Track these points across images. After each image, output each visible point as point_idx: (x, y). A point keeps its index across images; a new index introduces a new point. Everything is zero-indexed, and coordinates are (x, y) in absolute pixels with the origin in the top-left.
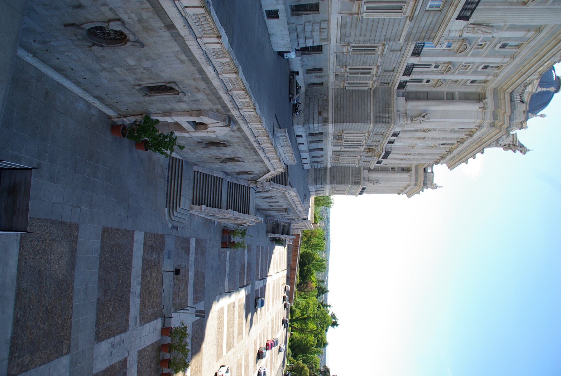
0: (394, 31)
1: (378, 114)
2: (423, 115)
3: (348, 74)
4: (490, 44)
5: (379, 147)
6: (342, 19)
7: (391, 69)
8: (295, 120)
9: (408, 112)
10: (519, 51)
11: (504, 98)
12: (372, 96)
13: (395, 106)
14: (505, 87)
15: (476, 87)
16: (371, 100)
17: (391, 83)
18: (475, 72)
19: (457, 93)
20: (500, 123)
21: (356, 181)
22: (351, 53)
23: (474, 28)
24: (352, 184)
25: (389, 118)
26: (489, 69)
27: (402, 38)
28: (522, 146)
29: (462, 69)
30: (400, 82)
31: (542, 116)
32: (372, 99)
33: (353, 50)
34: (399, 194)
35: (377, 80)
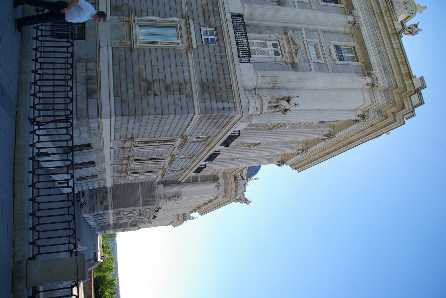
1: (145, 199)
2: (177, 196)
5: (148, 214)
8: (83, 210)
11: (231, 178)
12: (139, 186)
13: (157, 192)
14: (230, 172)
16: (139, 189)
19: (199, 177)
20: (230, 195)
21: (133, 224)
25: (153, 201)
28: (246, 199)
31: (256, 179)
32: (139, 188)
34: (167, 225)
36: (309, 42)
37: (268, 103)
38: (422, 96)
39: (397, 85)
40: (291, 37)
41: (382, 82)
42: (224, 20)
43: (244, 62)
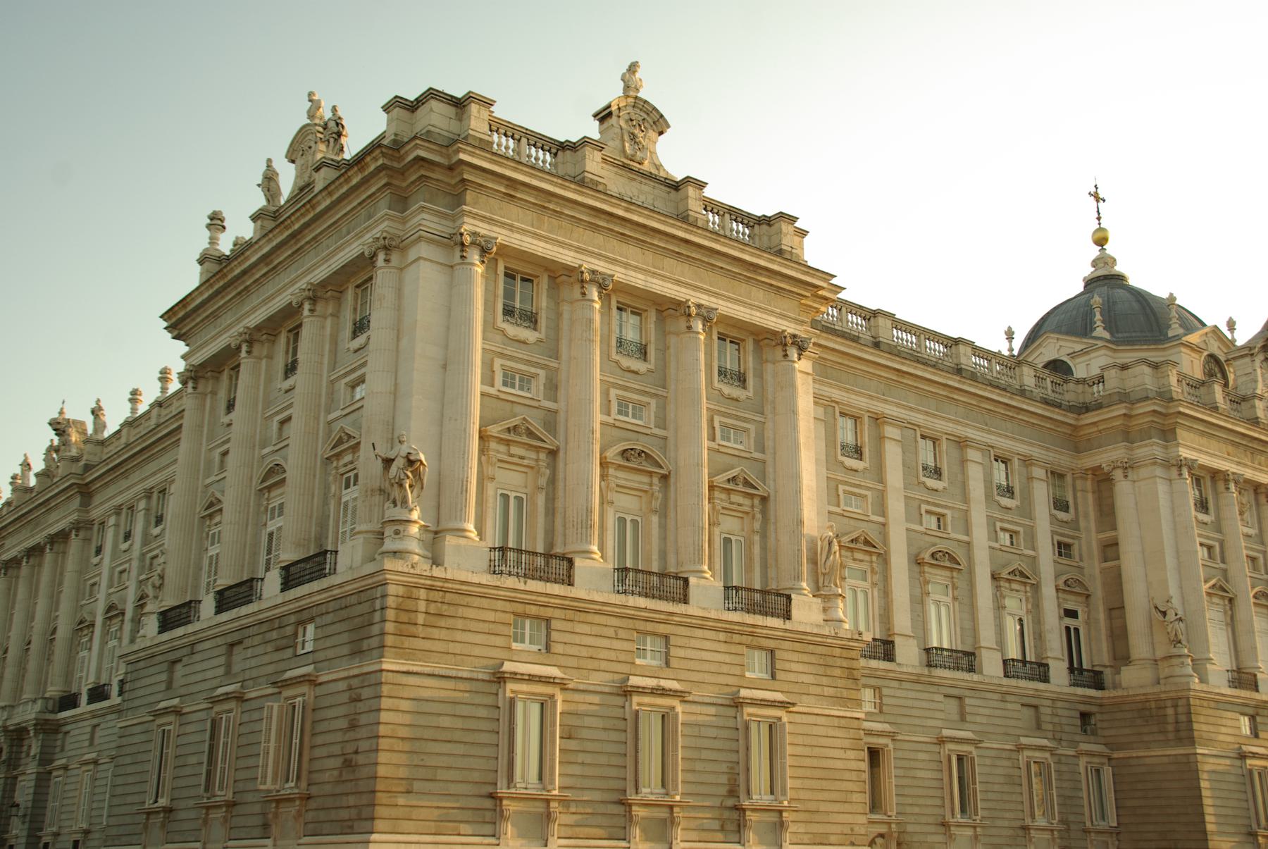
0: (831, 732)
1: (1171, 736)
3: (1053, 822)
4: (928, 503)
6: (800, 842)
7: (1028, 713)
9: (1159, 654)
11: (1094, 424)
12: (1128, 755)
15: (1079, 494)
17: (1083, 708)
18: (1027, 510)
19: (1101, 536)
22: (974, 817)
23: (824, 575)
25: (1175, 706)
26: (1012, 481)
27: (848, 714)
29: (1018, 544)
30: (1074, 684)
32: (1134, 755)
33: (963, 810)
35: (1073, 744)
36: (344, 403)
37: (395, 505)
38: (420, 96)
39: (385, 185)
40: (332, 448)
41: (382, 224)
42: (286, 608)
43: (335, 563)
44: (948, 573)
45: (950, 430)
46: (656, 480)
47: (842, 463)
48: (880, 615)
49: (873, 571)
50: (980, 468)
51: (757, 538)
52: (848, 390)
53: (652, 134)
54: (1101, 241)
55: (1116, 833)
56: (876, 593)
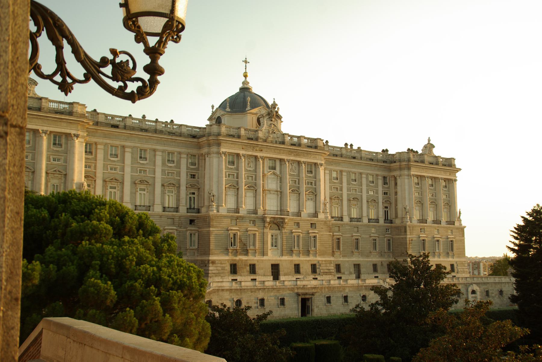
10: (148, 149)
17: (191, 218)
18: (178, 166)
24: (406, 235)
35: (185, 228)
44: (146, 186)
45: (150, 147)
46: (30, 173)
47: (110, 160)
48: (120, 198)
49: (118, 187)
50: (161, 157)
51: (62, 184)
52: (112, 140)
53: (33, 86)
54: (246, 76)
55: (198, 249)
56: (119, 192)
